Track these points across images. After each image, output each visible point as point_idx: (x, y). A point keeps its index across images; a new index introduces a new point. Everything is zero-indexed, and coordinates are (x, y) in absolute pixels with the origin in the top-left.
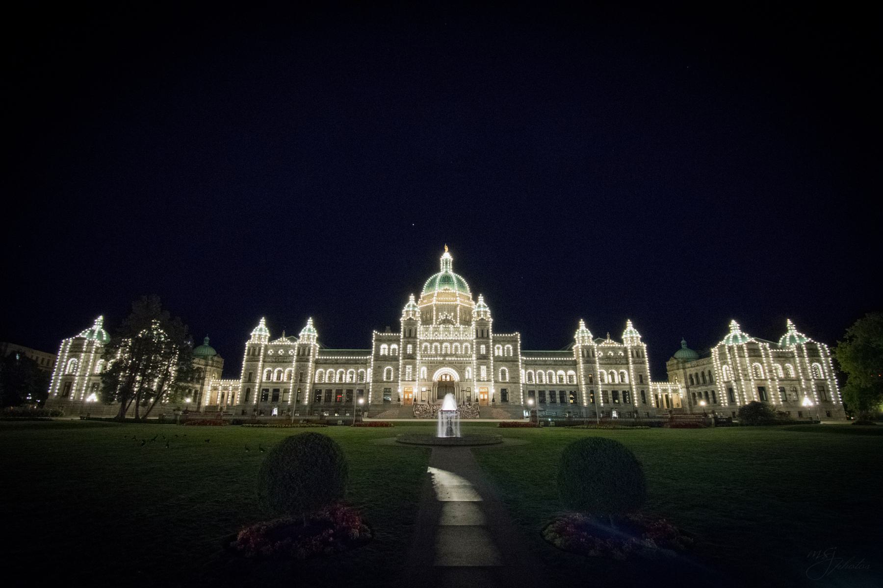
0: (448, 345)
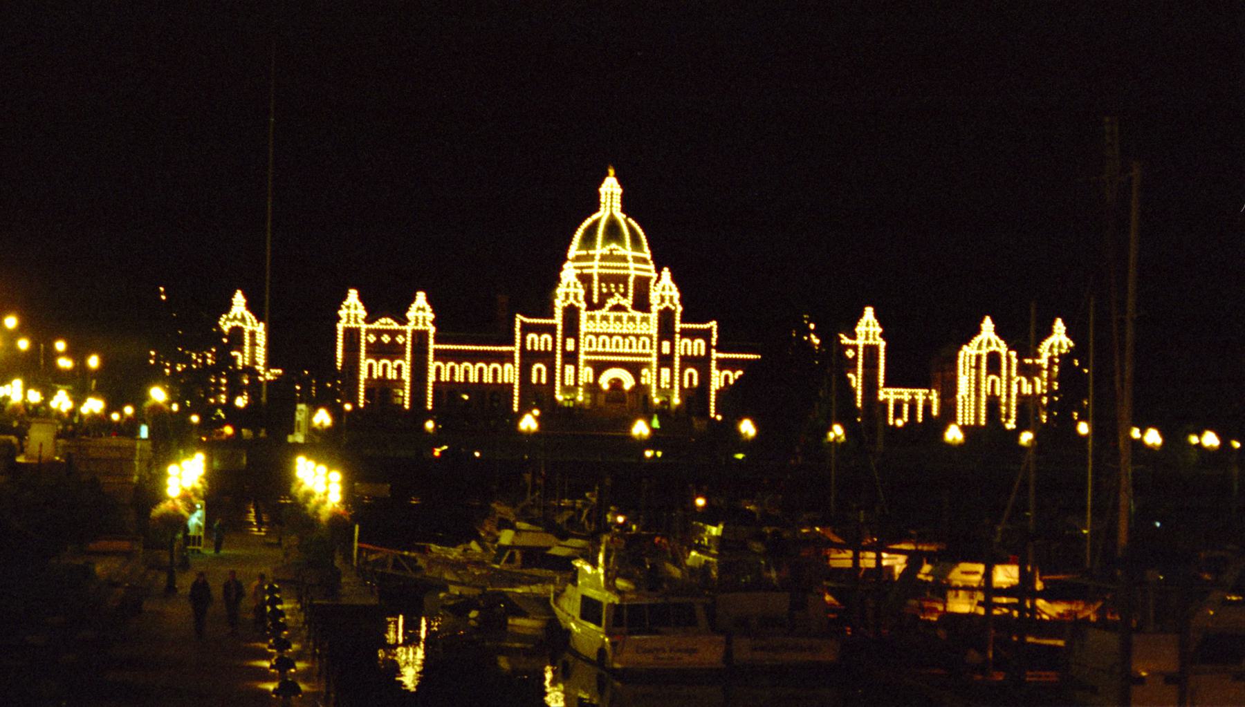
0: (620, 339)
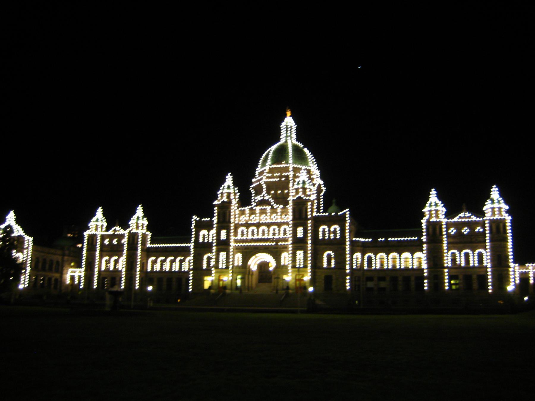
0: (265, 228)
